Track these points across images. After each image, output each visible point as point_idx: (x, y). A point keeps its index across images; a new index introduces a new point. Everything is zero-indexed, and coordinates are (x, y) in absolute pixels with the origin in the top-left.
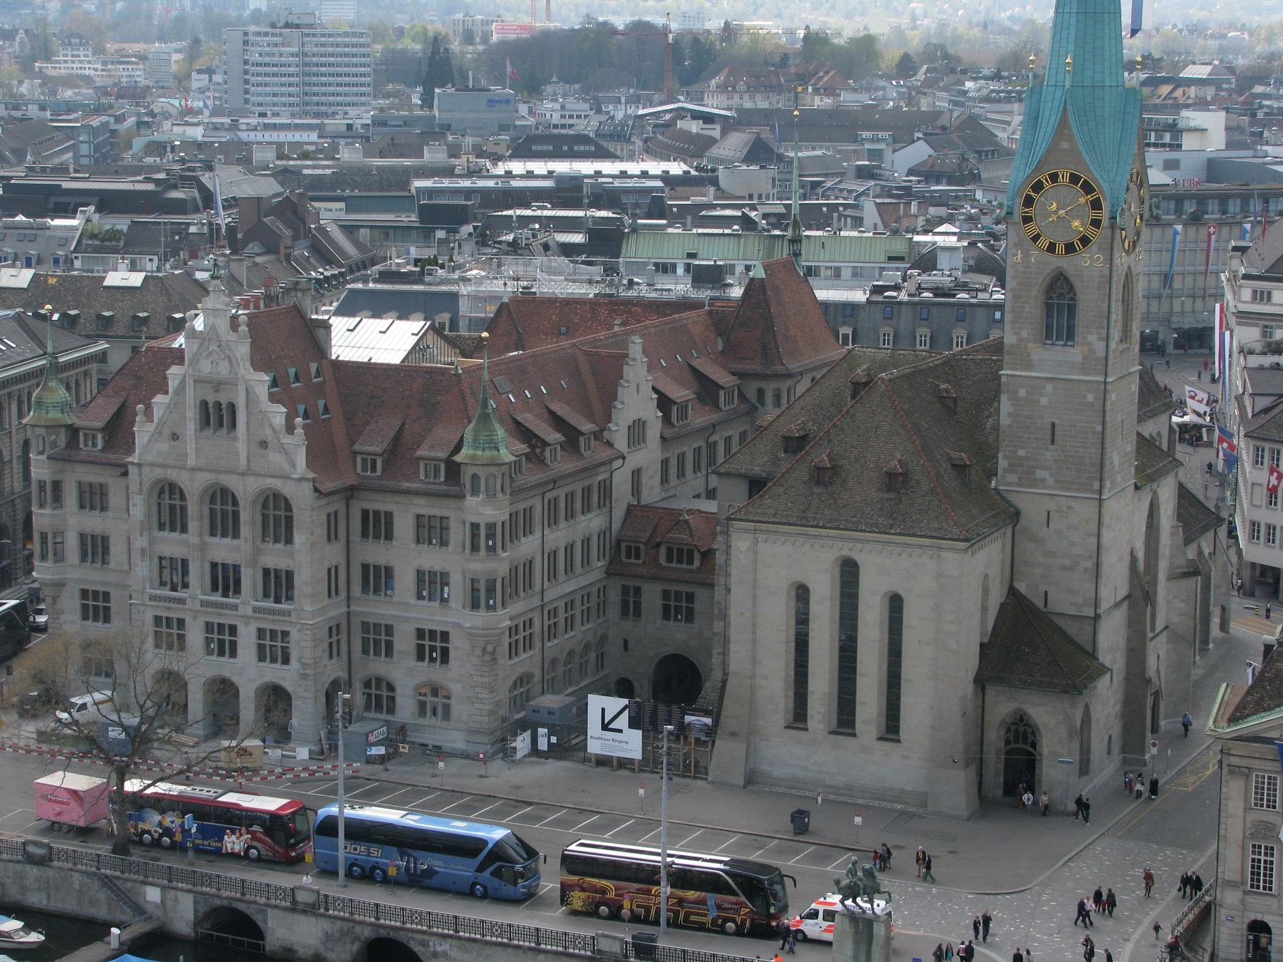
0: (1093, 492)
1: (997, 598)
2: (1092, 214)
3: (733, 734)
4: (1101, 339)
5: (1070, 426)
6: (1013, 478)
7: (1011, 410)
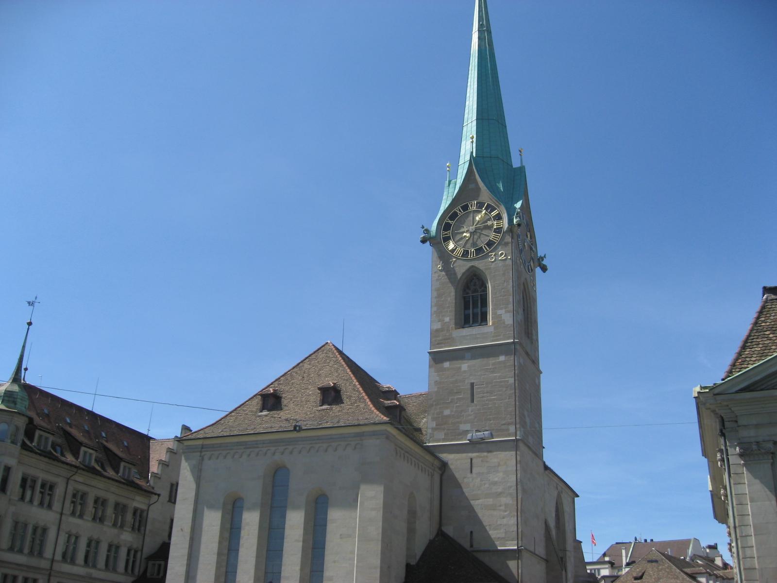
0: (509, 435)
1: (425, 532)
4: (509, 312)
6: (442, 435)
7: (437, 379)
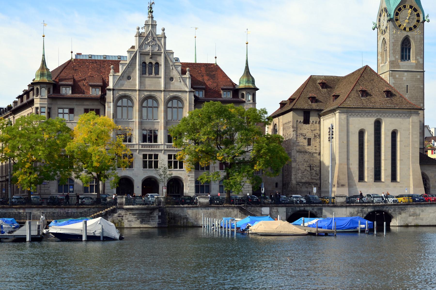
2: (416, 18)
3: (343, 185)
5: (413, 86)
7: (394, 82)
